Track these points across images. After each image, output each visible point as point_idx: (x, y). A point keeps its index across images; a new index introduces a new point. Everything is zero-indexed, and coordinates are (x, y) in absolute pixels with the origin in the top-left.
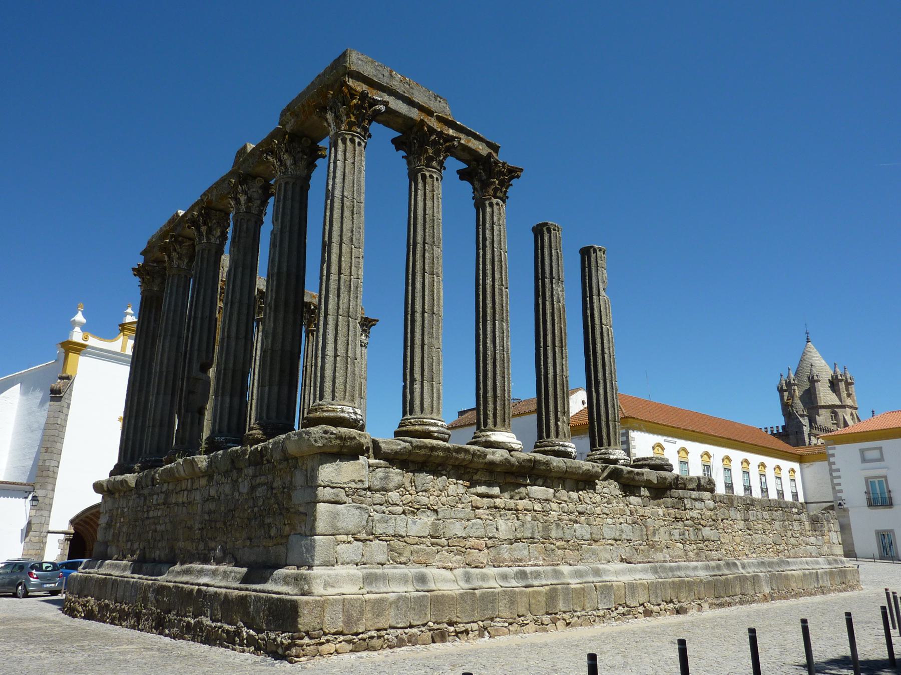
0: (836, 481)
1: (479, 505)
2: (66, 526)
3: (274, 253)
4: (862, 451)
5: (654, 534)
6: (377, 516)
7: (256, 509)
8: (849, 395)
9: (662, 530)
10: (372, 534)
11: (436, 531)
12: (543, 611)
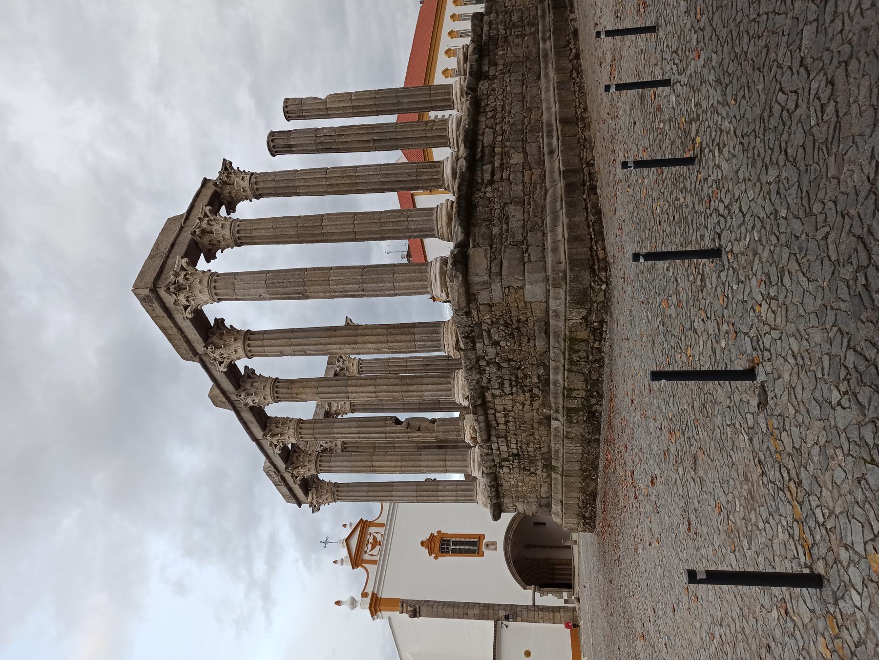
2: (529, 592)
5: (518, 57)
6: (510, 240)
9: (514, 51)
10: (523, 242)
11: (519, 202)
12: (576, 128)
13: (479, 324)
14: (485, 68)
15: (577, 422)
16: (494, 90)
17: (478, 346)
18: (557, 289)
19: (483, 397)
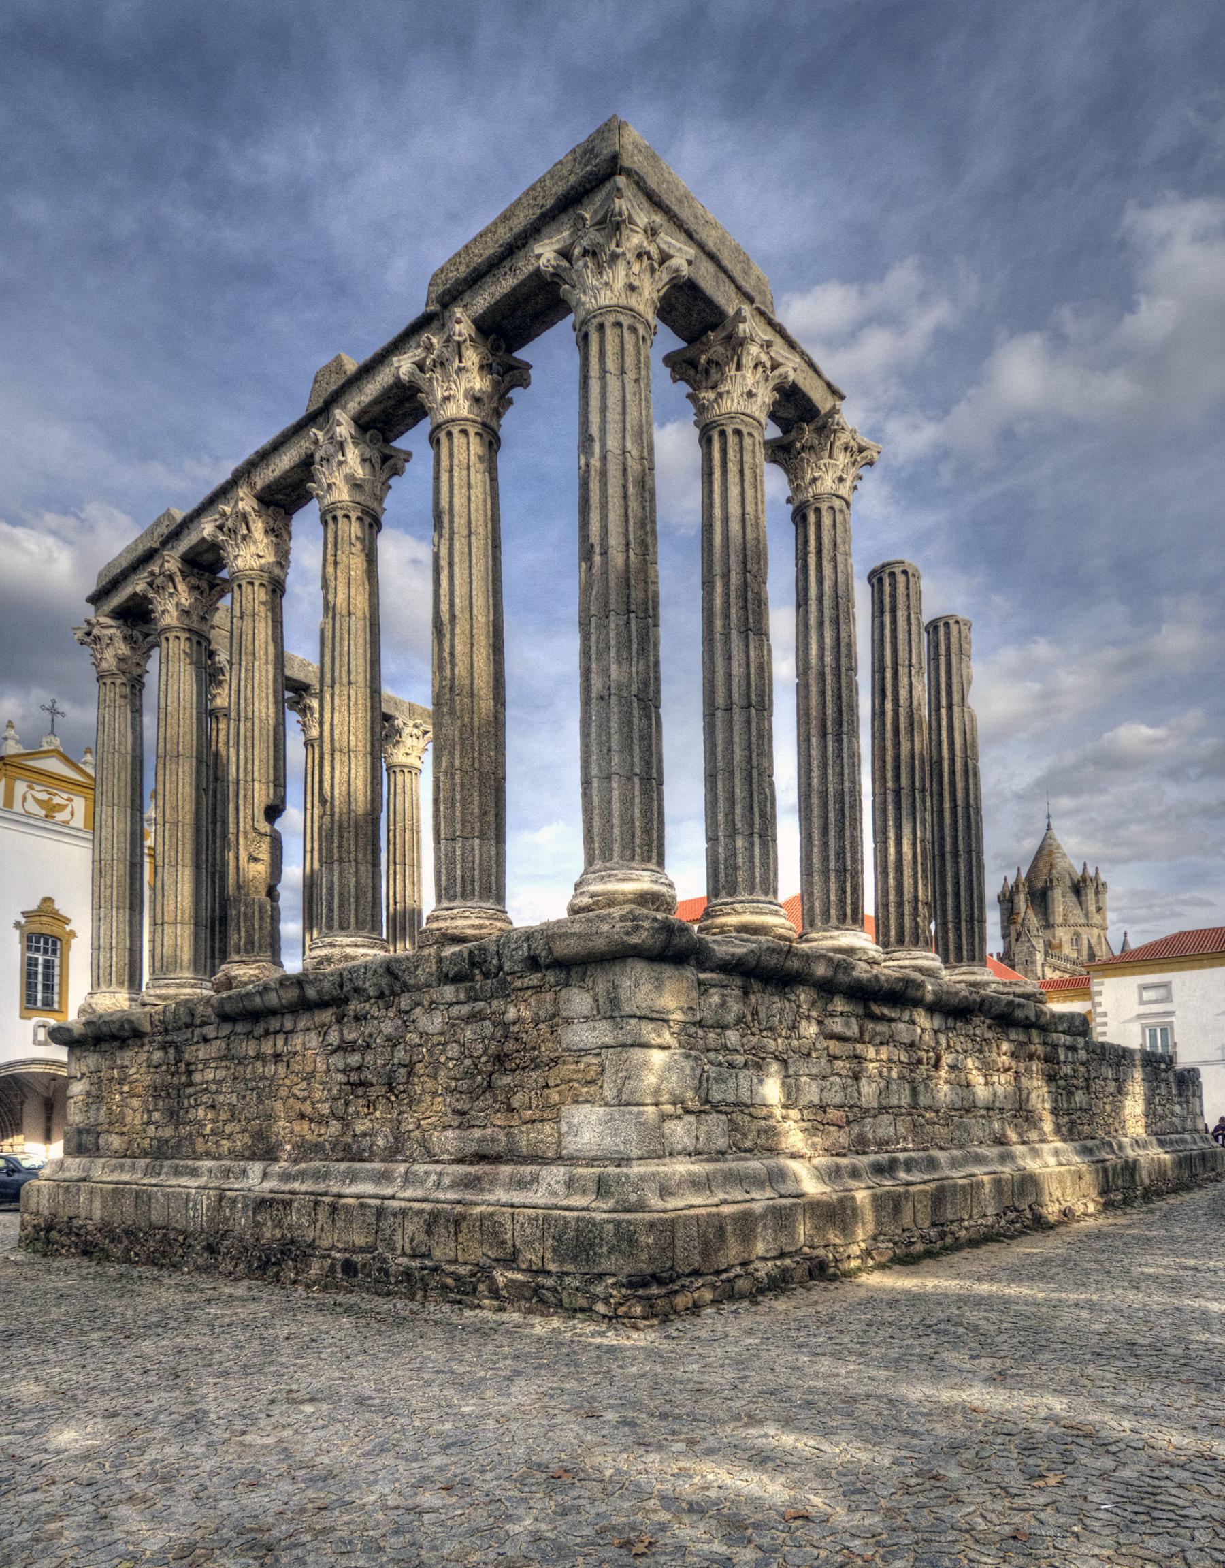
1: (838, 1053)
6: (712, 1071)
7: (468, 1062)
8: (1099, 909)
10: (707, 1101)
12: (927, 1224)
13: (504, 992)
15: (257, 1224)
17: (449, 992)
18: (592, 1186)
19: (322, 1005)
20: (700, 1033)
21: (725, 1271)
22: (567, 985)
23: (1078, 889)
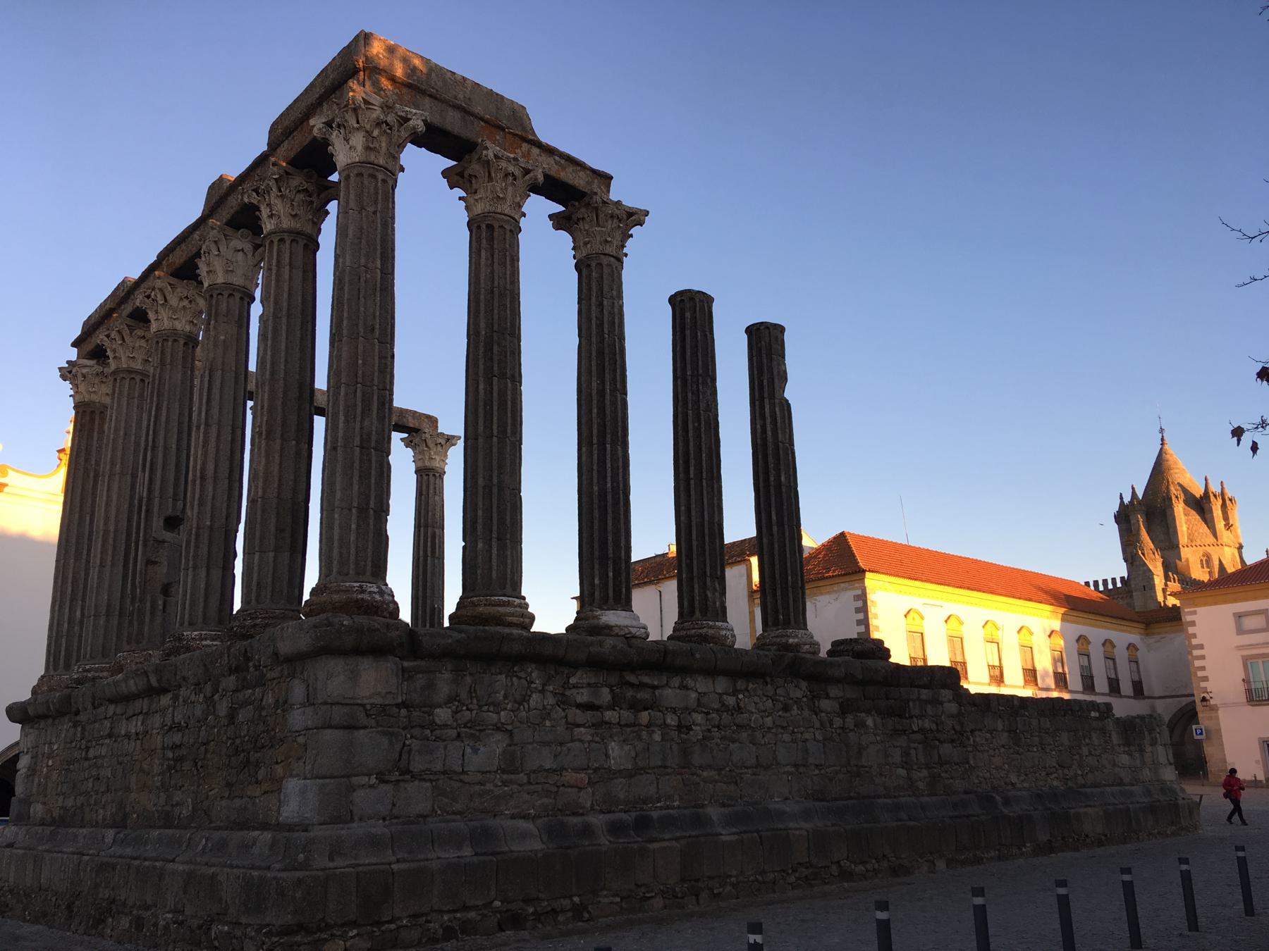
0: (1198, 663)
1: (579, 720)
3: (265, 350)
4: (1239, 616)
6: (415, 744)
7: (238, 741)
14: (834, 691)
16: (786, 708)
20: (404, 712)
21: (390, 922)
22: (292, 676)
23: (1201, 505)
